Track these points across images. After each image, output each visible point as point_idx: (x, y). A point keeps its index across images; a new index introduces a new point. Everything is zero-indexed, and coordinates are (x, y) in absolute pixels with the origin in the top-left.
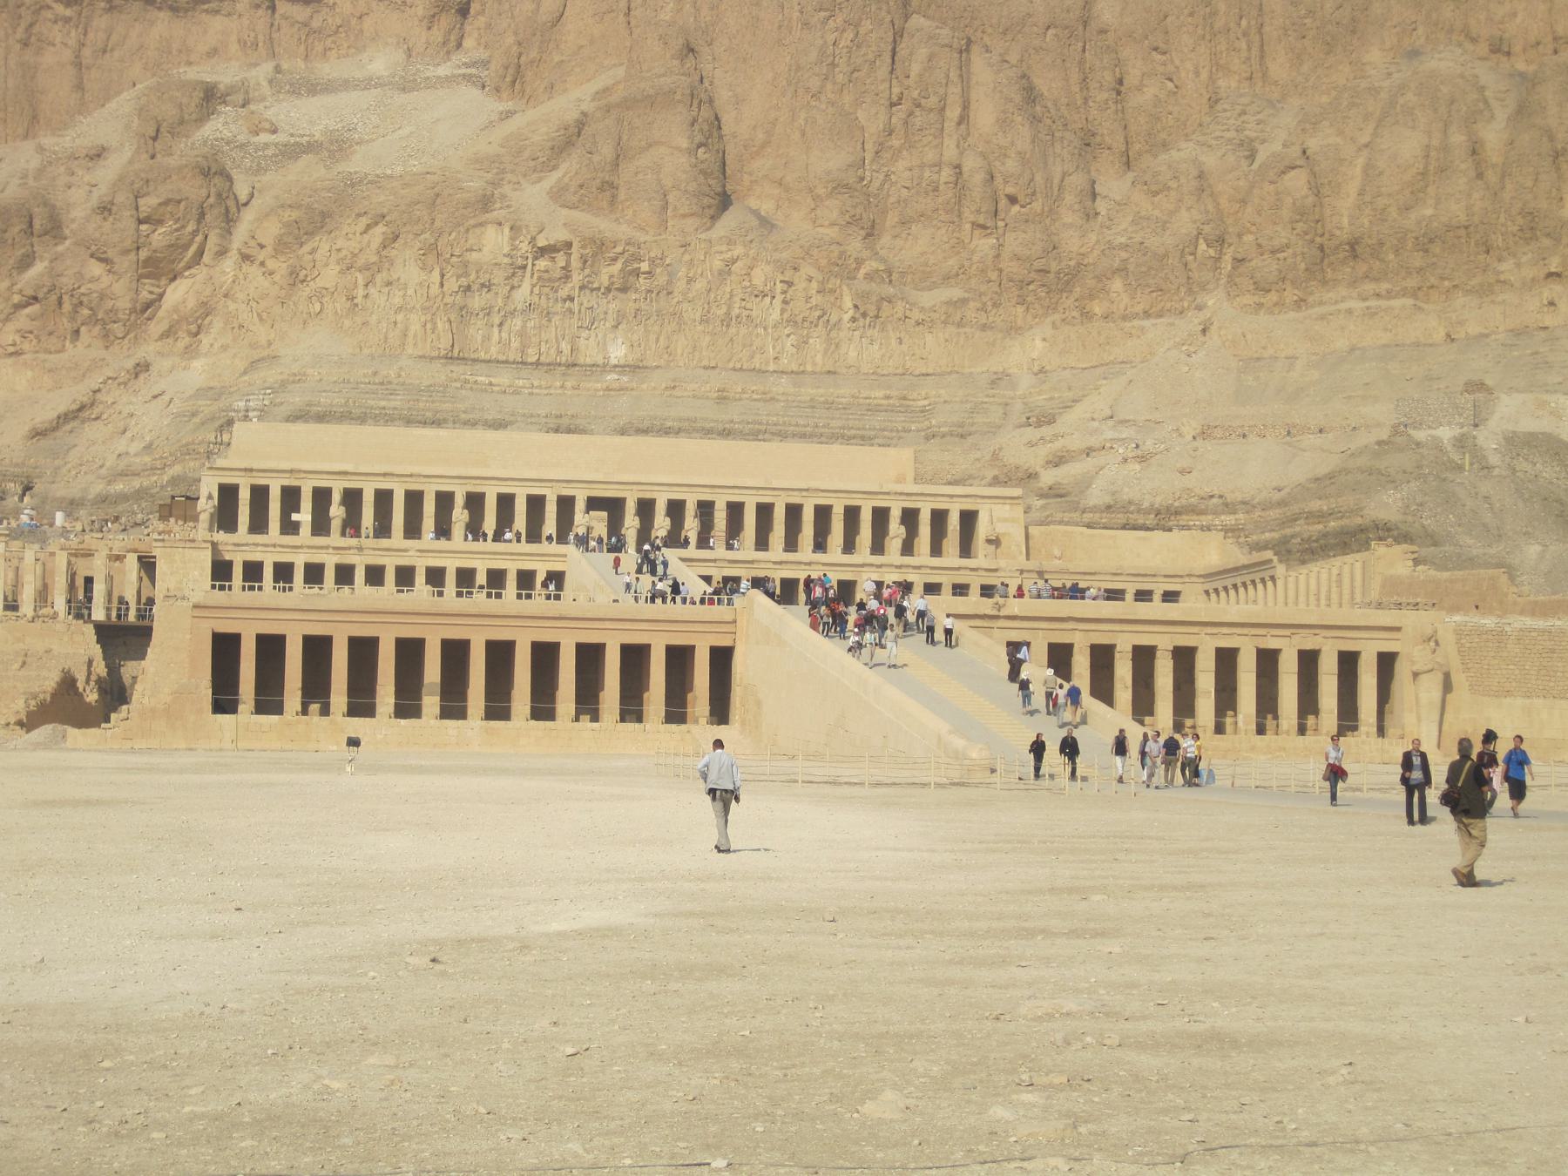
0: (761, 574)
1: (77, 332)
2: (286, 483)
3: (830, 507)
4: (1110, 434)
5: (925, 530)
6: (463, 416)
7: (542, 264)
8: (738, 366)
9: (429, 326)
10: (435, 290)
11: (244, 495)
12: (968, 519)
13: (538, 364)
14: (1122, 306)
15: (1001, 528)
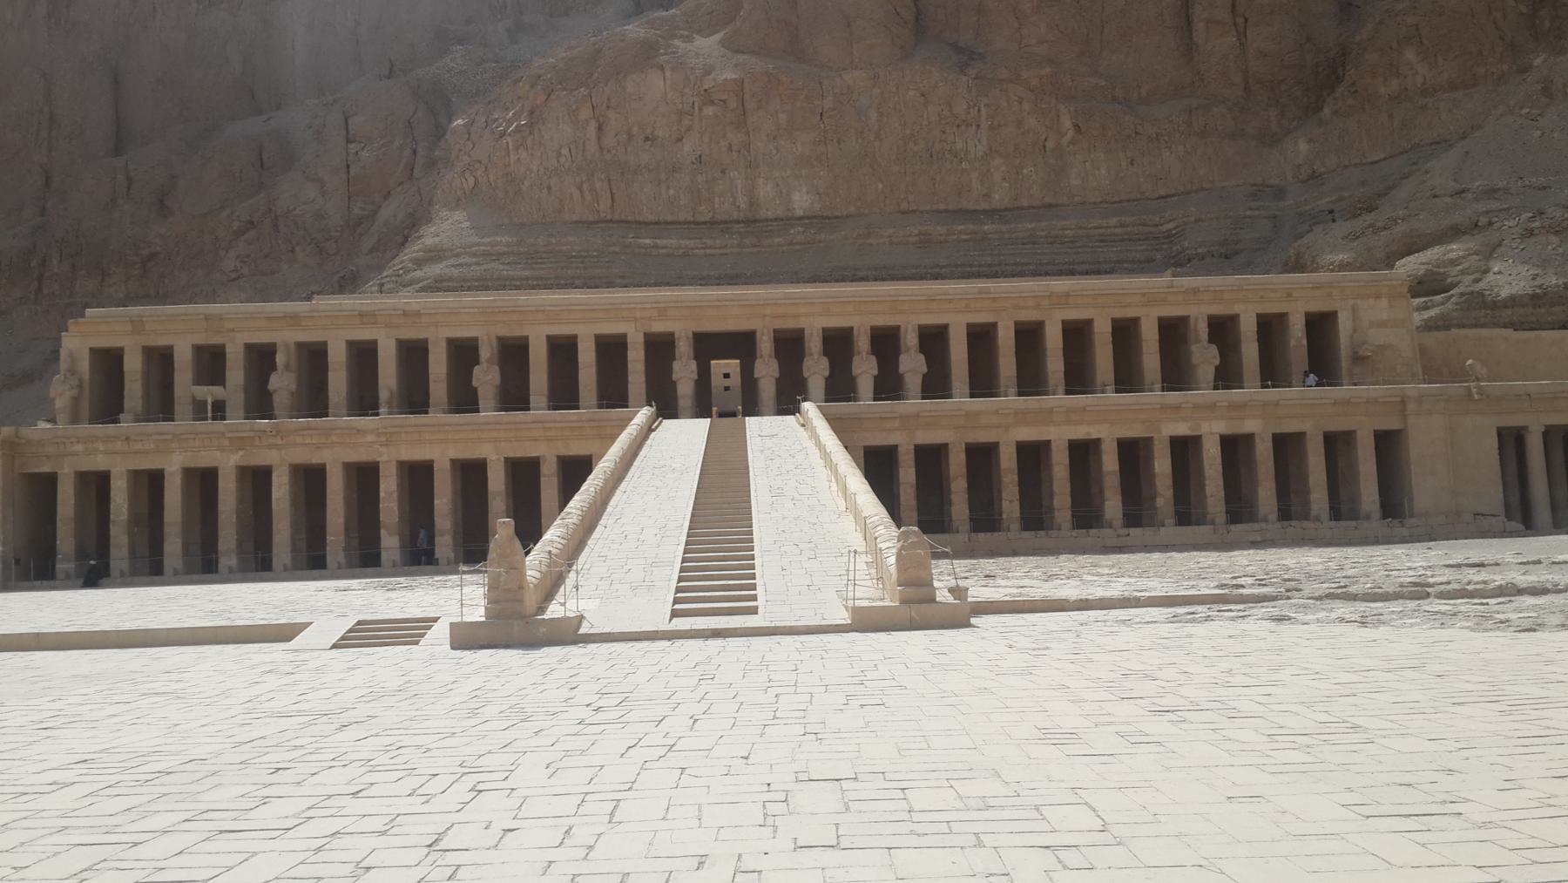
0: (984, 437)
1: (293, 251)
2: (201, 340)
3: (1089, 322)
4: (1481, 207)
5: (1250, 351)
6: (618, 281)
7: (709, 111)
8: (942, 207)
9: (585, 187)
10: (592, 148)
11: (133, 364)
12: (1320, 326)
13: (713, 223)
14: (1419, 80)
15: (1377, 337)
